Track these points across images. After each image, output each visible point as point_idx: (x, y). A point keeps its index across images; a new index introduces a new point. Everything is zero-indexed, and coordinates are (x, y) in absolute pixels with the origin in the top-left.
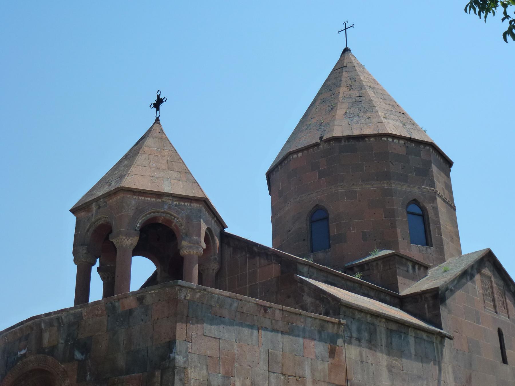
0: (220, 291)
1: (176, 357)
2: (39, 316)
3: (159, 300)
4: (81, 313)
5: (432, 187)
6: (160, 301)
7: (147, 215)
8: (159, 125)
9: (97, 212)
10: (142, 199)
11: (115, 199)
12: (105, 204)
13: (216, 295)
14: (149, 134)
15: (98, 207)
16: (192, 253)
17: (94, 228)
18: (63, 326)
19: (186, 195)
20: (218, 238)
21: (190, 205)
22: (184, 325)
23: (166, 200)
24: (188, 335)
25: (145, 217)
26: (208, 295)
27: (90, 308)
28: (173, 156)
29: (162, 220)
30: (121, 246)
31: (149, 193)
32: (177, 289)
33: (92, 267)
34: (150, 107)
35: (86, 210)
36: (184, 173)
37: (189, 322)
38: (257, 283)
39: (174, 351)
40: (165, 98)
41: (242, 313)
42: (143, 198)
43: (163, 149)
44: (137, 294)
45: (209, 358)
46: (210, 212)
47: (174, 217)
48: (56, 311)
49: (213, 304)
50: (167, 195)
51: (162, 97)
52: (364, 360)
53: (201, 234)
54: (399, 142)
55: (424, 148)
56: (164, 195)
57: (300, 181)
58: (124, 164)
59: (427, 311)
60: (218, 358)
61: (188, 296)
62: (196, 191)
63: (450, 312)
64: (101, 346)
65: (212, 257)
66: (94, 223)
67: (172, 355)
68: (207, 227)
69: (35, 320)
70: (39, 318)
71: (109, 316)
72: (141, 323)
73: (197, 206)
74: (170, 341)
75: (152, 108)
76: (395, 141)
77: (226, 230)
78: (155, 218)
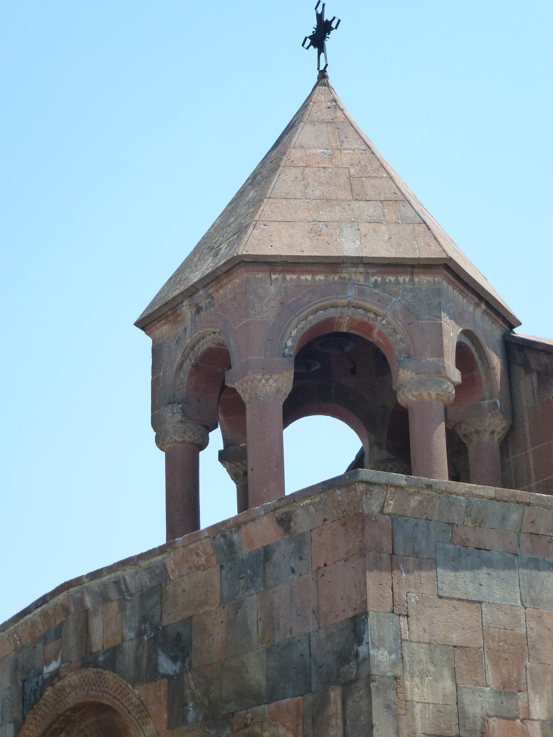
0: (469, 487)
1: (371, 652)
2: (77, 581)
3: (325, 520)
4: (165, 565)
6: (326, 522)
7: (307, 317)
8: (327, 88)
9: (193, 321)
10: (291, 279)
11: (230, 286)
12: (209, 300)
13: (463, 498)
14: (303, 115)
15: (195, 309)
16: (425, 395)
17: (192, 361)
18: (129, 598)
19: (398, 256)
20: (497, 355)
21: (412, 280)
22: (386, 576)
23: (351, 276)
24: (397, 598)
25: (303, 323)
26: (439, 497)
27: (181, 550)
28: (363, 163)
29: (346, 324)
30: (253, 395)
31: (308, 263)
32: (360, 491)
33: (201, 453)
34: (303, 45)
35: (171, 318)
36: (391, 202)
37: (399, 568)
39: (365, 641)
40: (334, 18)
41: (536, 534)
42: (295, 277)
43: (339, 147)
44: (275, 509)
45: (458, 651)
46: (467, 292)
47: (375, 314)
48: (111, 565)
49: (456, 519)
50: (352, 263)
51: (327, 17)
53: (445, 350)
56: (343, 263)
58: (247, 199)
60: (479, 648)
61: (390, 504)
62: (422, 244)
64: (213, 640)
65: (486, 402)
66: (192, 348)
67: (362, 649)
68: (461, 329)
69: (72, 589)
70: (78, 585)
71: (222, 567)
72: (292, 576)
73: (428, 282)
74: (354, 617)
75: (308, 48)
77: (519, 332)
78: (329, 322)
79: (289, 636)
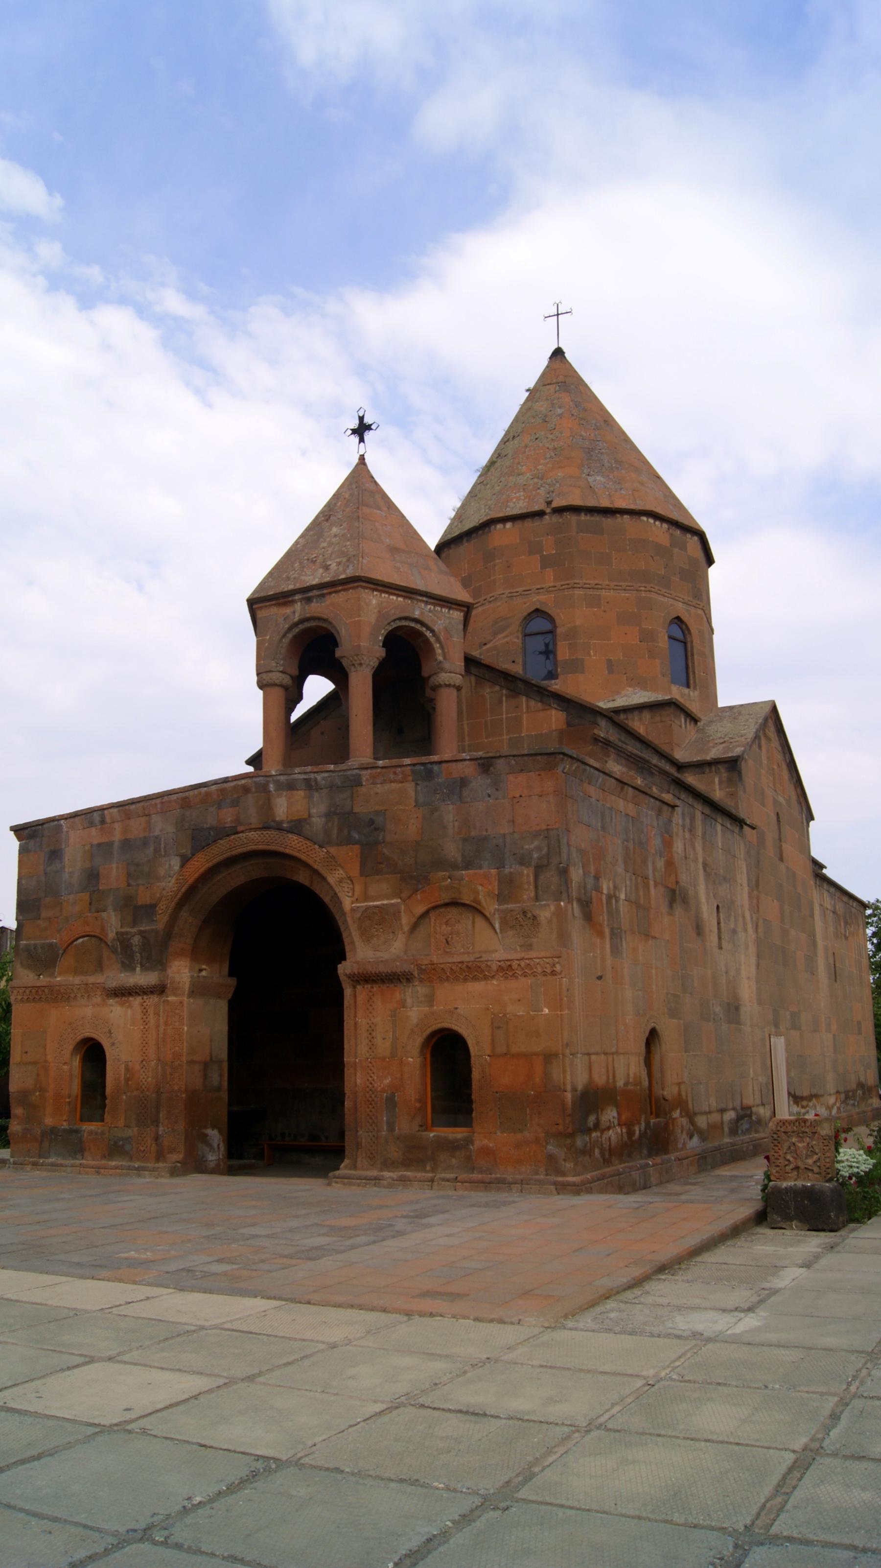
5: (698, 600)
38: (523, 735)
42: (387, 596)
51: (367, 420)
54: (661, 526)
55: (691, 539)
57: (509, 567)
59: (717, 787)
63: (745, 791)
66: (296, 624)
76: (658, 523)
79: (484, 833)
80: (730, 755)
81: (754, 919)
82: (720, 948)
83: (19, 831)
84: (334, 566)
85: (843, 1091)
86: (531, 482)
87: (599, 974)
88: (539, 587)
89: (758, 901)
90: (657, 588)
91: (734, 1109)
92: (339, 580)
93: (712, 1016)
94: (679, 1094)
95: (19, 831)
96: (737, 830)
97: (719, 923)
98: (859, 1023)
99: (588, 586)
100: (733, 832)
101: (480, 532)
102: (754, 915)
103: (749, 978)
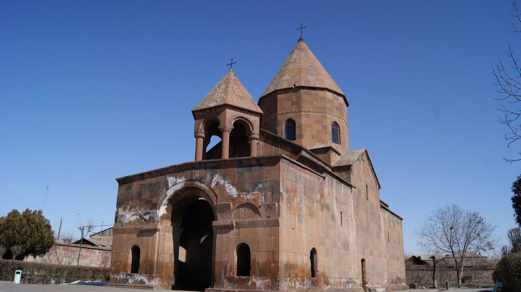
5: (342, 116)
52: (330, 194)
63: (353, 175)
80: (348, 164)
81: (356, 218)
82: (342, 225)
83: (118, 180)
84: (219, 101)
85: (391, 279)
86: (290, 79)
87: (293, 227)
88: (291, 111)
89: (358, 212)
90: (328, 112)
91: (345, 278)
92: (220, 105)
93: (337, 247)
94: (323, 271)
95: (118, 180)
96: (349, 188)
97: (341, 217)
98: (398, 257)
99: (306, 111)
100: (348, 189)
101: (273, 94)
102: (356, 216)
103: (353, 236)
